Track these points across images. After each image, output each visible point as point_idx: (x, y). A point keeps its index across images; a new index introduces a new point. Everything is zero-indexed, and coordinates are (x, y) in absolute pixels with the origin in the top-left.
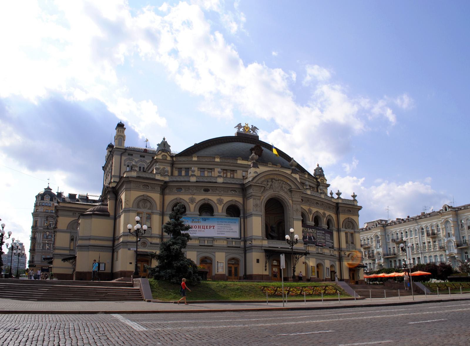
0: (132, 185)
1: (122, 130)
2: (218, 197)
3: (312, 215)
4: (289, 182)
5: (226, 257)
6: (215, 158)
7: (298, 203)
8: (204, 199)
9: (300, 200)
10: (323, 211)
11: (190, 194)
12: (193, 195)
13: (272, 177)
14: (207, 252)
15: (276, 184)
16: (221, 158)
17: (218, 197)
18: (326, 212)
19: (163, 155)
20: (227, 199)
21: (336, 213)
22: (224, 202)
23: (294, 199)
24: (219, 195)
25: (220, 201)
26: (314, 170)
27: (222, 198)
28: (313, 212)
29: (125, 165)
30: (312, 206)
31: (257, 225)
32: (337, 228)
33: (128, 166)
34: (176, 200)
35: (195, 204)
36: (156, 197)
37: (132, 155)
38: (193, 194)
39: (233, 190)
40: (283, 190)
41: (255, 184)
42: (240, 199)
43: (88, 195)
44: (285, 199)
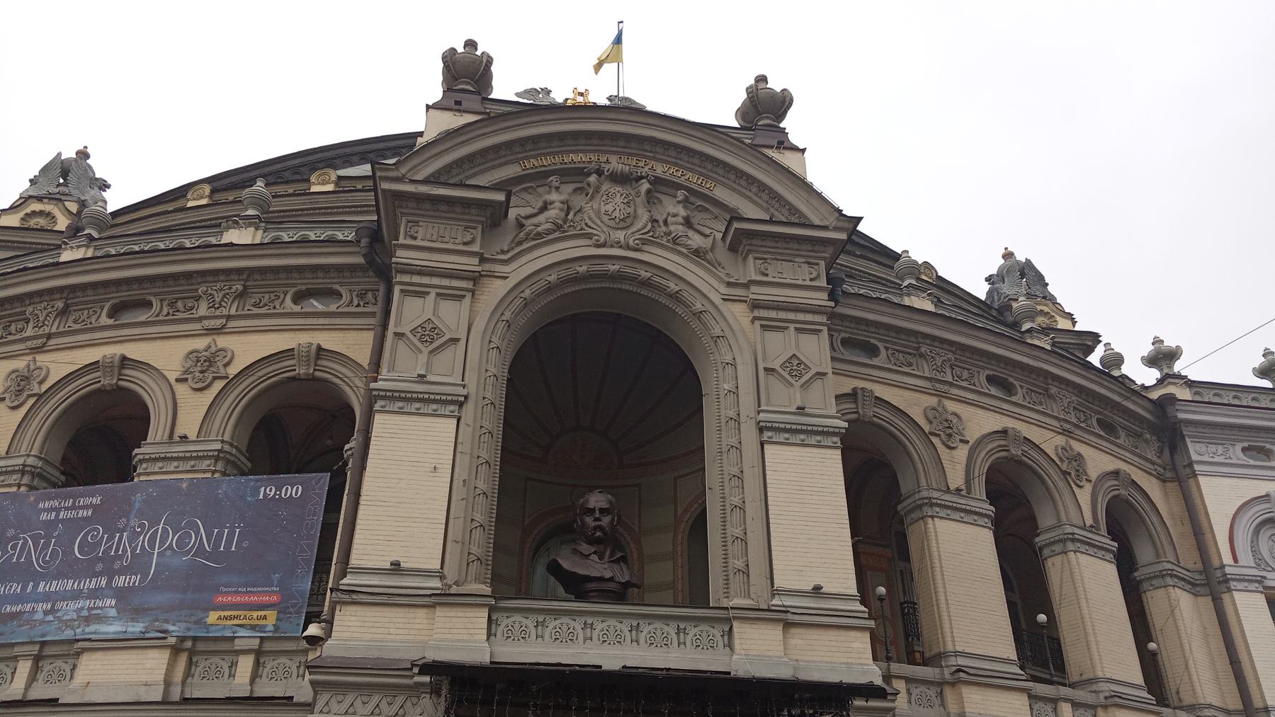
2: (200, 343)
3: (962, 453)
4: (721, 193)
7: (800, 317)
8: (94, 366)
9: (821, 298)
10: (1060, 440)
11: (22, 346)
13: (577, 158)
15: (614, 201)
16: (343, 183)
17: (200, 343)
18: (1078, 447)
21: (1169, 475)
22: (233, 370)
23: (757, 293)
24: (206, 323)
26: (987, 279)
28: (973, 434)
30: (954, 391)
31: (416, 486)
32: (1199, 566)
35: (31, 401)
38: (39, 342)
39: (312, 285)
40: (675, 241)
41: (424, 189)
44: (687, 295)
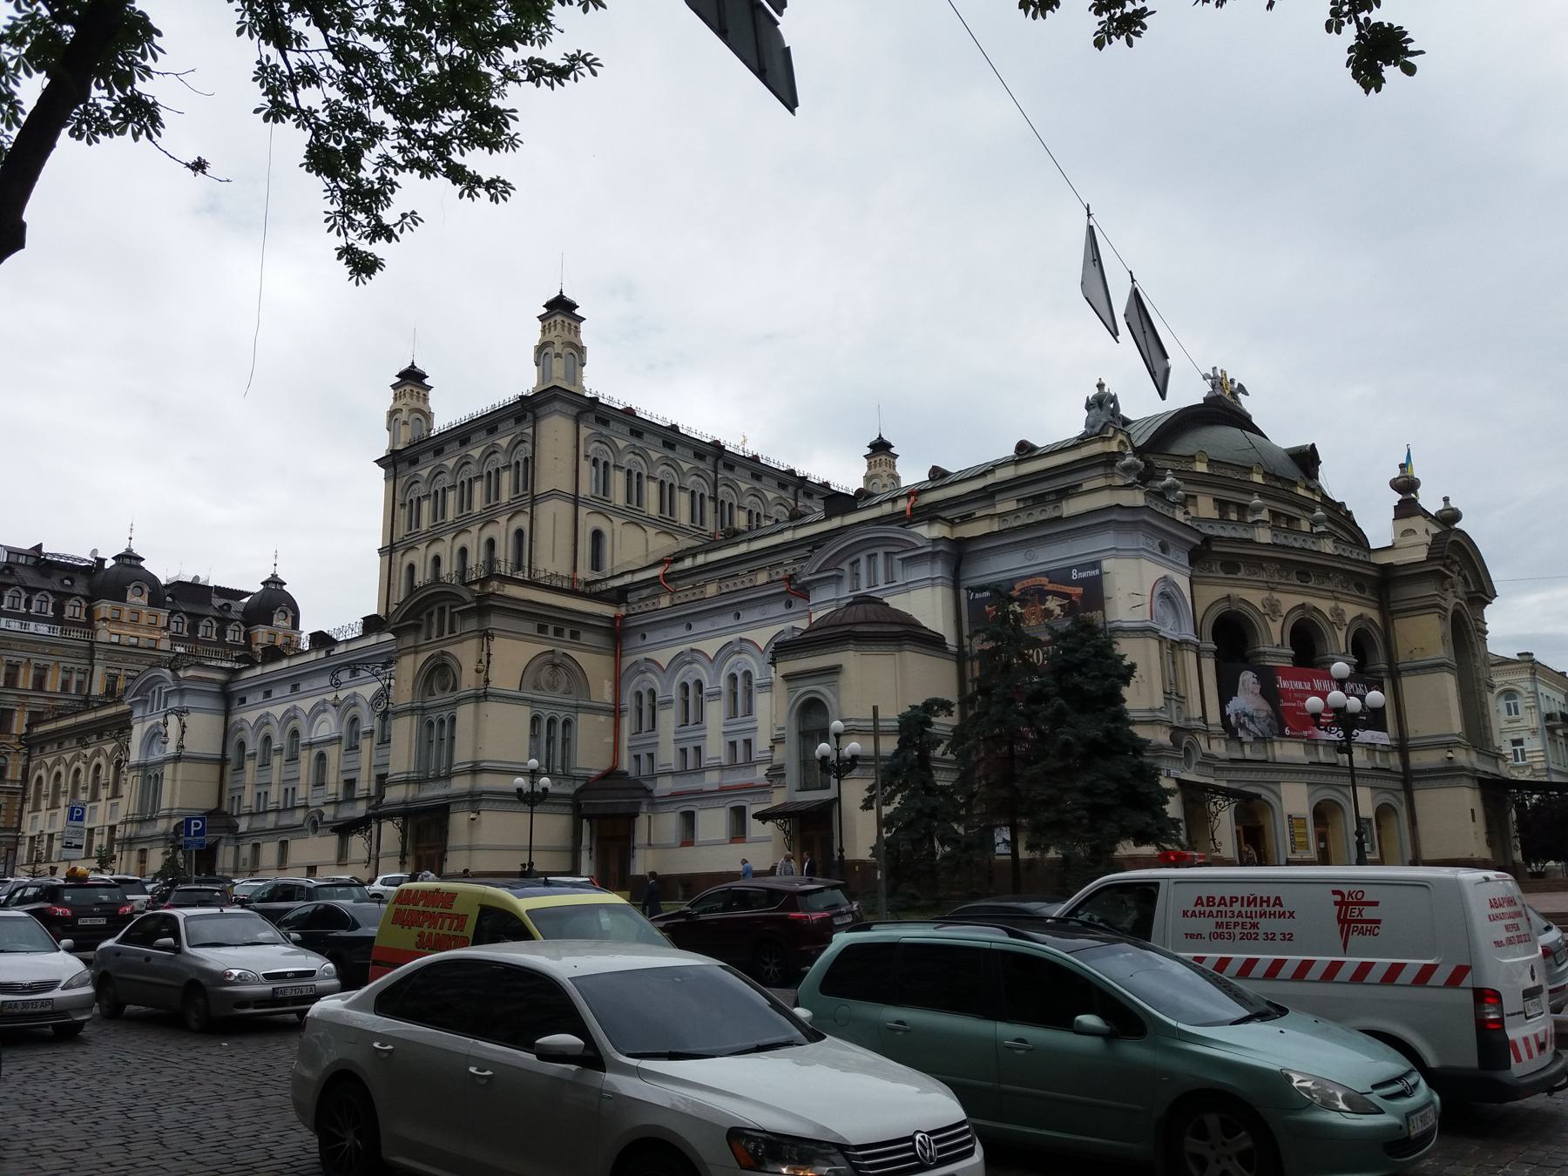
0: (1140, 540)
1: (574, 324)
5: (1373, 799)
6: (1249, 470)
8: (1303, 606)
12: (1272, 589)
14: (1329, 786)
17: (1332, 604)
19: (1121, 442)
20: (1351, 611)
25: (1339, 614)
27: (1342, 605)
29: (587, 456)
33: (595, 462)
34: (1226, 604)
35: (1281, 620)
36: (1183, 582)
37: (605, 423)
42: (1374, 615)
43: (44, 550)
